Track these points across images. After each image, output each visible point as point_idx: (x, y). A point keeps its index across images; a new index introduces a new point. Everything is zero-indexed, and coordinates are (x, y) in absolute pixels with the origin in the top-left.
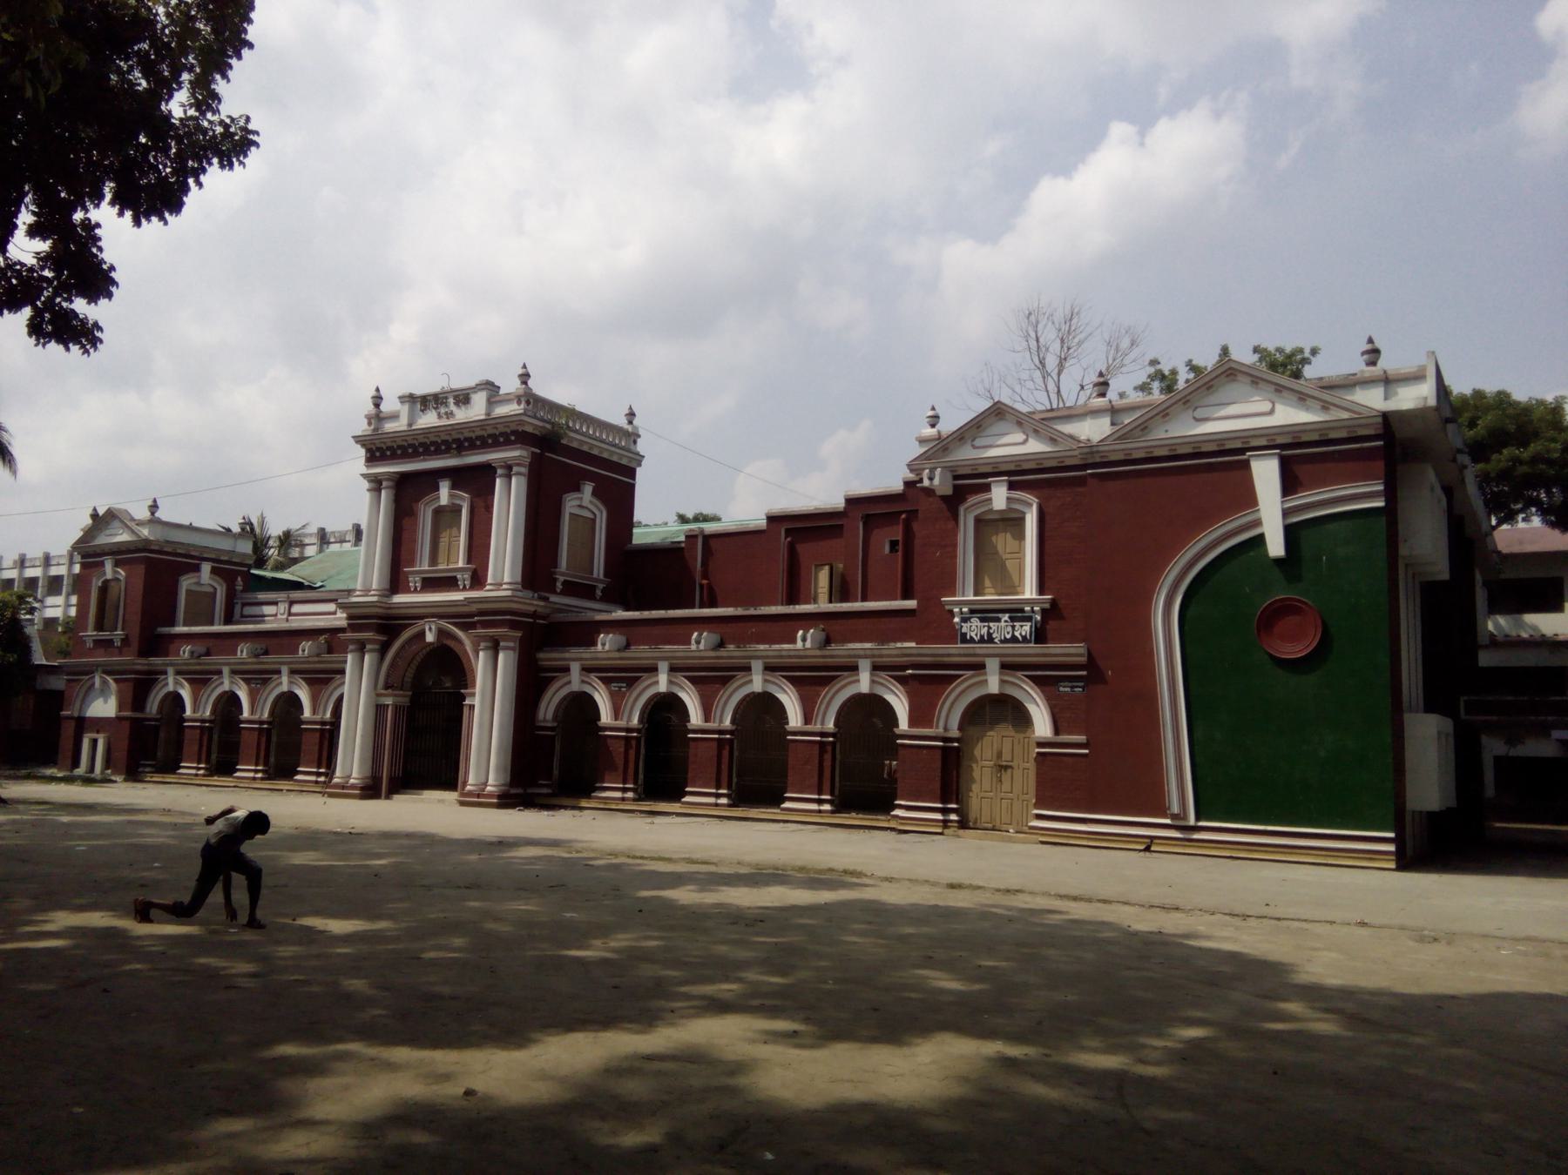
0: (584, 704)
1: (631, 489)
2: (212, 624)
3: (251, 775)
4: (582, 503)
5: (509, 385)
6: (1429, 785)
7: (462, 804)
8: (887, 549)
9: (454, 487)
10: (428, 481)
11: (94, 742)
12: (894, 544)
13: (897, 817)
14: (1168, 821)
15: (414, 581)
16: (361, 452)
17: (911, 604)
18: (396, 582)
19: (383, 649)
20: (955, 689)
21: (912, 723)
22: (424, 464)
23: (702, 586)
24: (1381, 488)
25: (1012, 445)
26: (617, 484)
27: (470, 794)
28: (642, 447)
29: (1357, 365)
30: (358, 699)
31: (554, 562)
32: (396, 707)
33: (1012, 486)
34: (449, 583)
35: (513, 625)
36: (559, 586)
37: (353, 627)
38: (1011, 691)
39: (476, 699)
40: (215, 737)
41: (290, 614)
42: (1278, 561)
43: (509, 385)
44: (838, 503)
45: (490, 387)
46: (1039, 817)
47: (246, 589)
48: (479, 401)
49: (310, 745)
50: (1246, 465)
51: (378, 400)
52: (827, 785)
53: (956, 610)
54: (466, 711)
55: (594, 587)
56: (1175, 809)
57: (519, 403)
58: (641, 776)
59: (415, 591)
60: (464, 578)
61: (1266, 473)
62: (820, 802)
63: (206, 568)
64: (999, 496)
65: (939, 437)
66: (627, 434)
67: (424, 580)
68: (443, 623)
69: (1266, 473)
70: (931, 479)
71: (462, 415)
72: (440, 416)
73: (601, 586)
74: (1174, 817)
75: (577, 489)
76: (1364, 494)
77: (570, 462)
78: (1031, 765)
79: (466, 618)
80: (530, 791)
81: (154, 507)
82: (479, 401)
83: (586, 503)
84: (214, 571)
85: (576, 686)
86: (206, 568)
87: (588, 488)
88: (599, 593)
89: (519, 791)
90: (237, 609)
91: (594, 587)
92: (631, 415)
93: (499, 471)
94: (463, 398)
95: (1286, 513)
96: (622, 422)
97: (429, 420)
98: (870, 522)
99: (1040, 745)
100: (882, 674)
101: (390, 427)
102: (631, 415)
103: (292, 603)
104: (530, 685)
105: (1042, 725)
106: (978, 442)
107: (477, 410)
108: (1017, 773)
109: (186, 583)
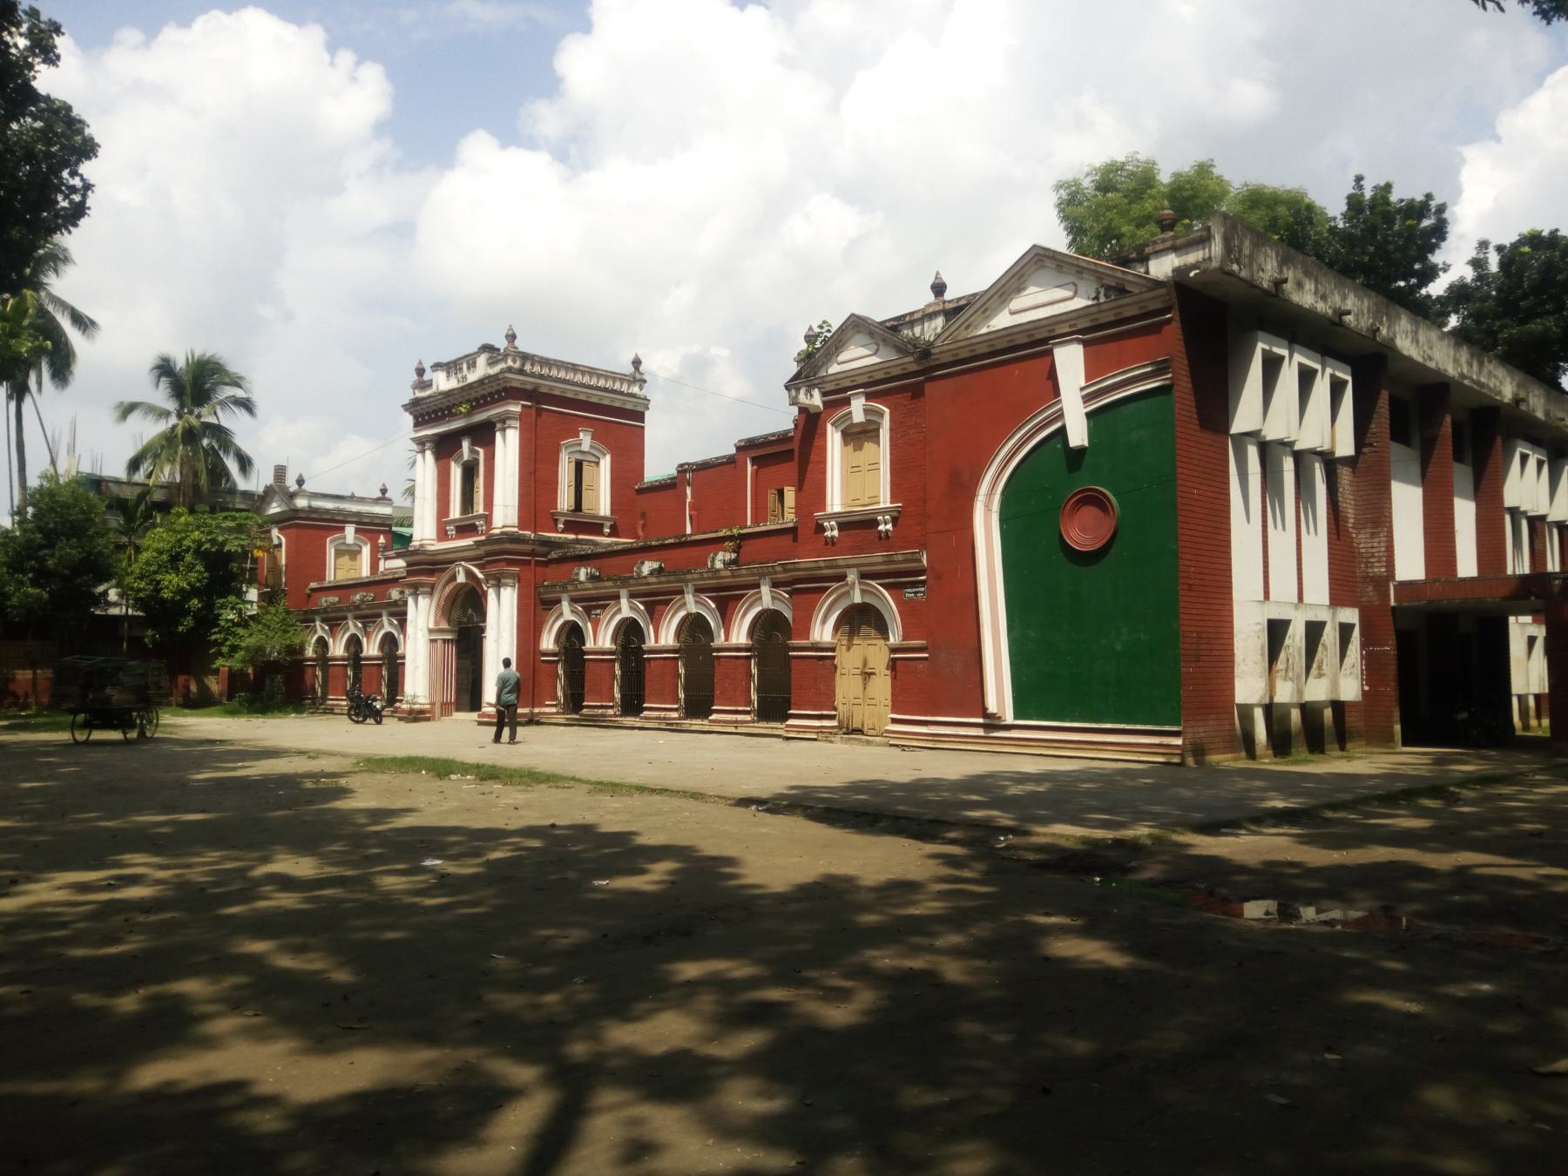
7: (480, 723)
9: (474, 443)
16: (409, 419)
25: (857, 357)
37: (410, 573)
42: (1081, 451)
43: (501, 344)
46: (894, 721)
48: (482, 360)
50: (1050, 353)
61: (1070, 361)
63: (350, 531)
64: (858, 408)
69: (1070, 361)
74: (992, 716)
80: (537, 710)
82: (482, 360)
84: (357, 531)
88: (607, 530)
94: (470, 360)
96: (630, 369)
102: (637, 363)
106: (841, 358)
107: (482, 369)
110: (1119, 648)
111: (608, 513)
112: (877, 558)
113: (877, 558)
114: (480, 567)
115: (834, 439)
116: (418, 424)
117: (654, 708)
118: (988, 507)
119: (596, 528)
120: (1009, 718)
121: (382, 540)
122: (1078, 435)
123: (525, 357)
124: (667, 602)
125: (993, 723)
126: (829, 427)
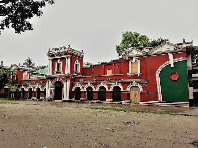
4: (77, 62)
5: (67, 47)
11: (13, 95)
12: (118, 67)
15: (55, 73)
17: (123, 74)
18: (53, 73)
19: (51, 81)
22: (56, 58)
26: (81, 59)
27: (64, 100)
29: (182, 42)
30: (49, 88)
33: (136, 59)
34: (60, 73)
38: (137, 85)
39: (64, 88)
42: (172, 68)
43: (67, 47)
44: (111, 61)
49: (41, 94)
51: (49, 49)
53: (129, 75)
56: (160, 100)
60: (62, 72)
61: (171, 56)
63: (26, 72)
64: (134, 60)
69: (171, 56)
71: (61, 51)
74: (159, 101)
77: (76, 57)
78: (140, 95)
81: (19, 64)
85: (77, 86)
86: (26, 72)
87: (77, 60)
90: (30, 77)
92: (82, 51)
94: (61, 49)
95: (173, 61)
97: (57, 51)
98: (115, 63)
100: (119, 83)
102: (82, 51)
104: (72, 86)
105: (141, 90)
107: (63, 50)
108: (138, 96)
109: (23, 74)
110: (179, 92)
114: (62, 79)
116: (49, 57)
117: (94, 100)
118: (158, 73)
119: (78, 73)
122: (172, 66)
123: (71, 49)
124: (97, 85)
125: (160, 102)
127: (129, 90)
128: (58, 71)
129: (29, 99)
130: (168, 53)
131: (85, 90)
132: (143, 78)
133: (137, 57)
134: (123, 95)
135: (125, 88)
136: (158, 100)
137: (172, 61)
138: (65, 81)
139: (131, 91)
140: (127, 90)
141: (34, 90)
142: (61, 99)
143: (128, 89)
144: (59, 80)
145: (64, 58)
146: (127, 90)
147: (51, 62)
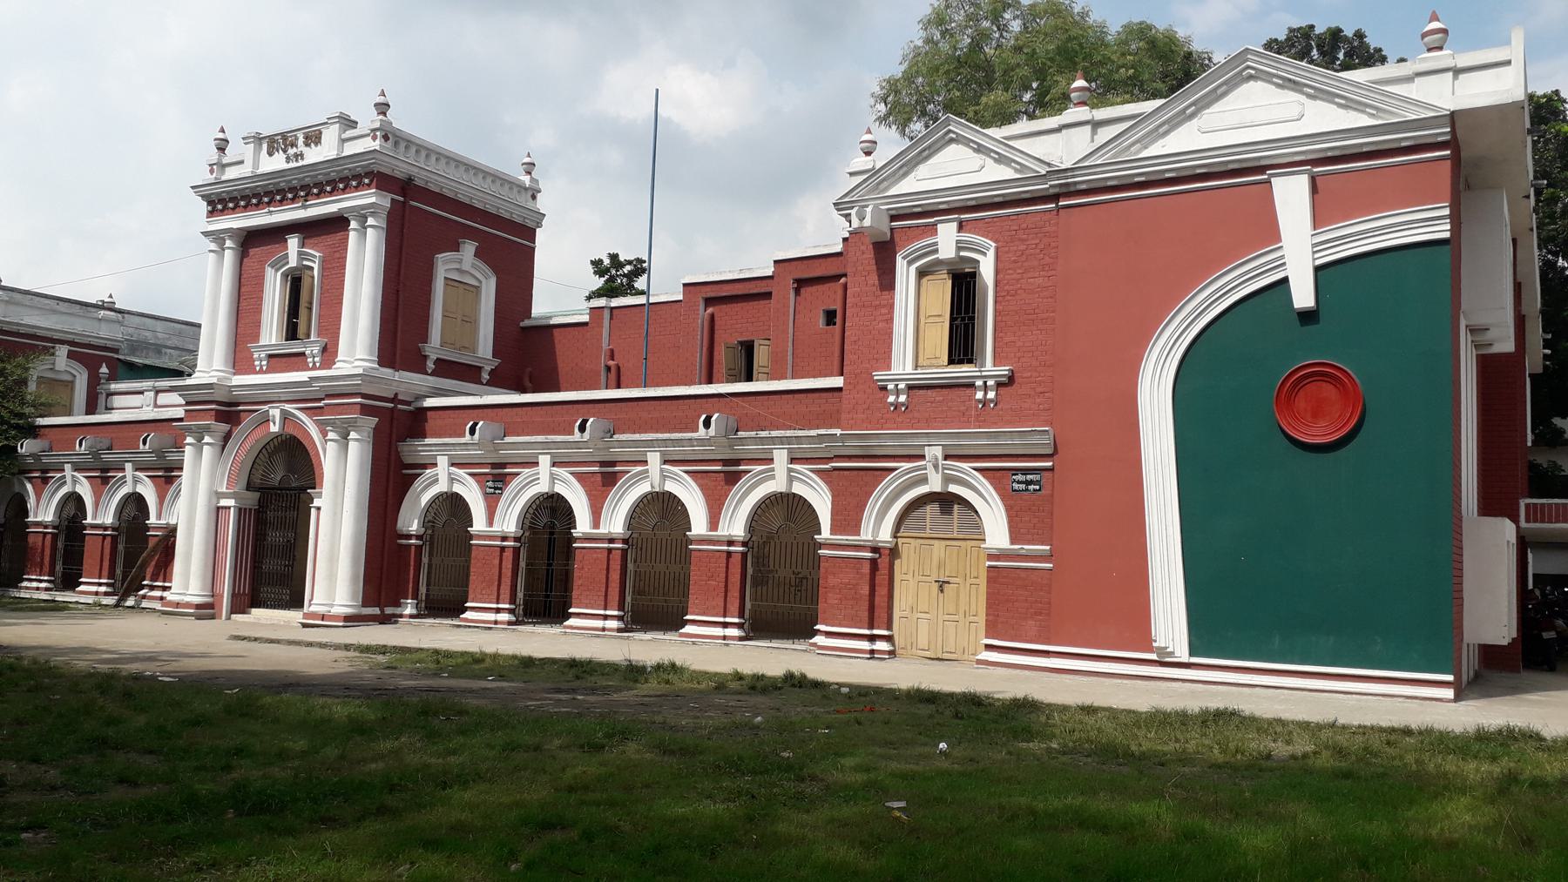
0: (454, 506)
1: (530, 253)
2: (70, 414)
3: (94, 589)
4: (458, 266)
5: (367, 119)
6: (1492, 615)
8: (821, 321)
9: (303, 245)
10: (276, 234)
13: (814, 645)
14: (1154, 657)
15: (259, 357)
16: (203, 207)
17: (838, 382)
18: (240, 359)
20: (887, 486)
21: (834, 531)
23: (608, 369)
24: (1447, 212)
26: (509, 244)
28: (542, 203)
31: (424, 337)
32: (241, 511)
34: (296, 360)
35: (366, 410)
36: (430, 365)
40: (60, 545)
41: (156, 406)
42: (1307, 316)
45: (348, 123)
46: (989, 647)
47: (113, 377)
48: (330, 135)
52: (734, 605)
54: (313, 511)
55: (480, 369)
57: (374, 138)
58: (520, 595)
59: (261, 372)
61: (1291, 196)
62: (725, 625)
65: (873, 172)
66: (522, 188)
67: (270, 356)
68: (287, 407)
69: (1291, 196)
70: (862, 219)
71: (313, 155)
72: (288, 160)
73: (488, 368)
74: (1162, 651)
75: (456, 248)
76: (1426, 223)
79: (316, 400)
83: (466, 266)
84: (71, 355)
86: (62, 351)
87: (469, 248)
88: (485, 376)
89: (376, 611)
90: (102, 399)
91: (480, 369)
93: (353, 224)
97: (277, 163)
99: (991, 557)
101: (231, 173)
102: (529, 168)
103: (157, 392)
104: (390, 479)
105: (996, 530)
111: (490, 356)
112: (976, 437)
113: (976, 437)
115: (905, 275)
120: (1183, 654)
121: (104, 369)
122: (1303, 296)
126: (899, 259)
127: (885, 535)
128: (295, 347)
129: (61, 597)
130: (1261, 169)
131: (509, 522)
132: (1018, 417)
133: (970, 209)
134: (831, 581)
135: (847, 518)
136: (1146, 642)
137: (1298, 252)
138: (331, 435)
139: (908, 548)
140: (866, 534)
141: (102, 515)
142: (296, 601)
143: (878, 527)
144: (291, 430)
145: (337, 224)
146: (866, 534)
147: (229, 256)
